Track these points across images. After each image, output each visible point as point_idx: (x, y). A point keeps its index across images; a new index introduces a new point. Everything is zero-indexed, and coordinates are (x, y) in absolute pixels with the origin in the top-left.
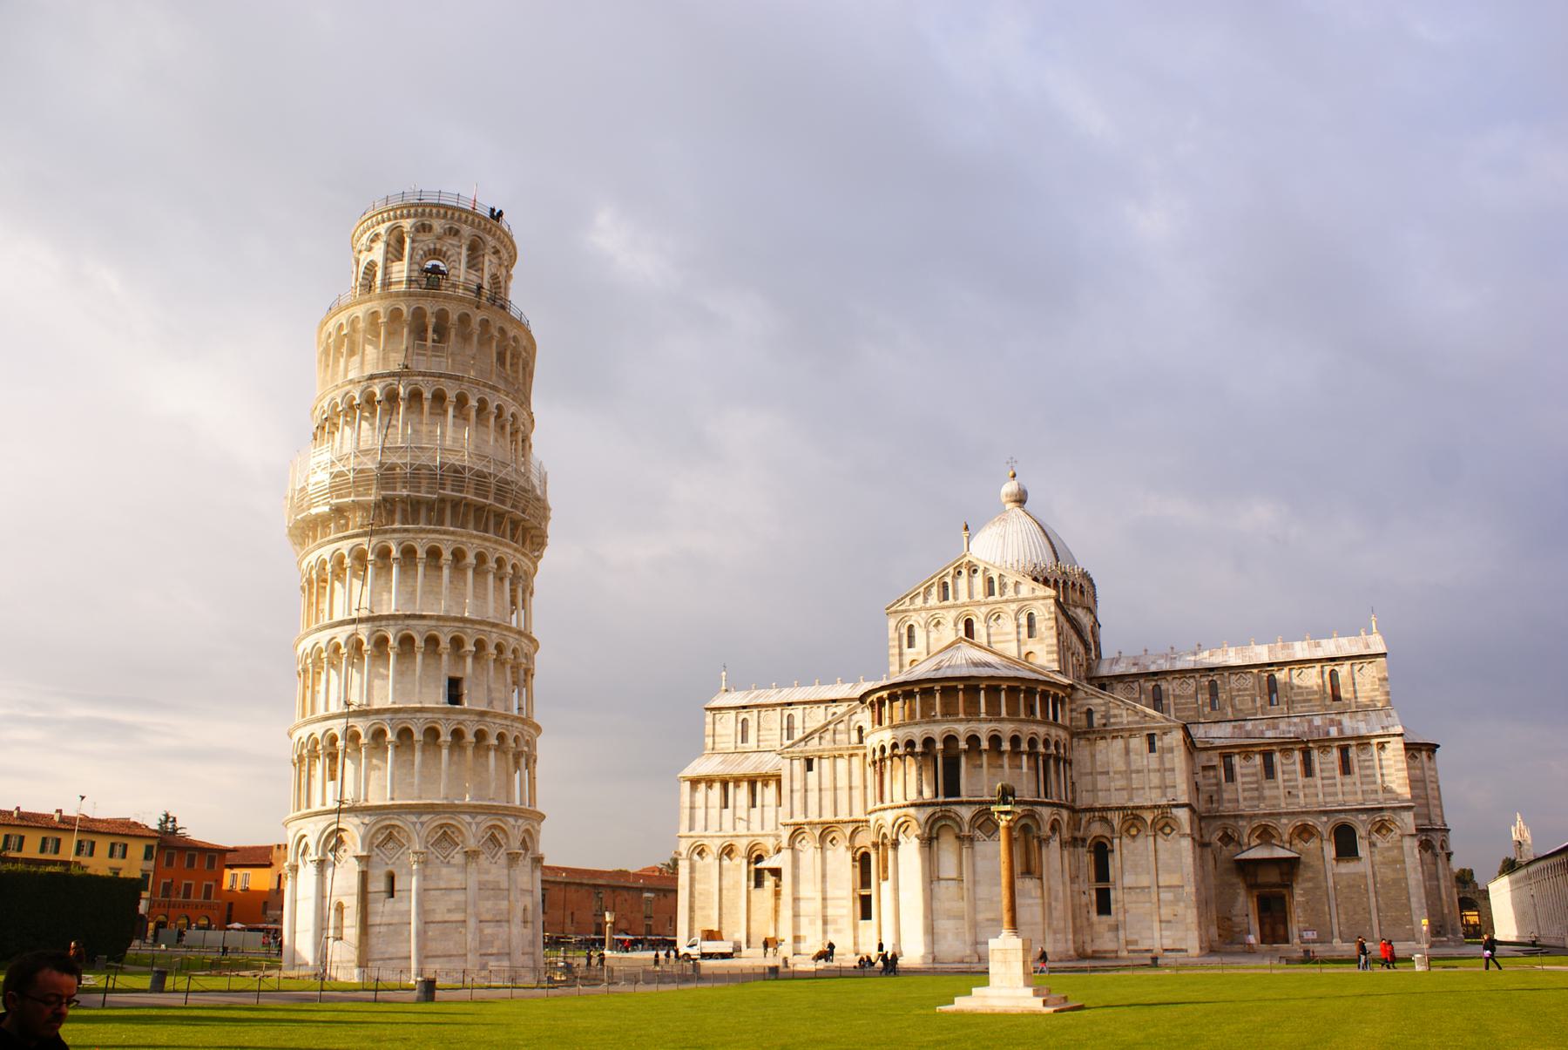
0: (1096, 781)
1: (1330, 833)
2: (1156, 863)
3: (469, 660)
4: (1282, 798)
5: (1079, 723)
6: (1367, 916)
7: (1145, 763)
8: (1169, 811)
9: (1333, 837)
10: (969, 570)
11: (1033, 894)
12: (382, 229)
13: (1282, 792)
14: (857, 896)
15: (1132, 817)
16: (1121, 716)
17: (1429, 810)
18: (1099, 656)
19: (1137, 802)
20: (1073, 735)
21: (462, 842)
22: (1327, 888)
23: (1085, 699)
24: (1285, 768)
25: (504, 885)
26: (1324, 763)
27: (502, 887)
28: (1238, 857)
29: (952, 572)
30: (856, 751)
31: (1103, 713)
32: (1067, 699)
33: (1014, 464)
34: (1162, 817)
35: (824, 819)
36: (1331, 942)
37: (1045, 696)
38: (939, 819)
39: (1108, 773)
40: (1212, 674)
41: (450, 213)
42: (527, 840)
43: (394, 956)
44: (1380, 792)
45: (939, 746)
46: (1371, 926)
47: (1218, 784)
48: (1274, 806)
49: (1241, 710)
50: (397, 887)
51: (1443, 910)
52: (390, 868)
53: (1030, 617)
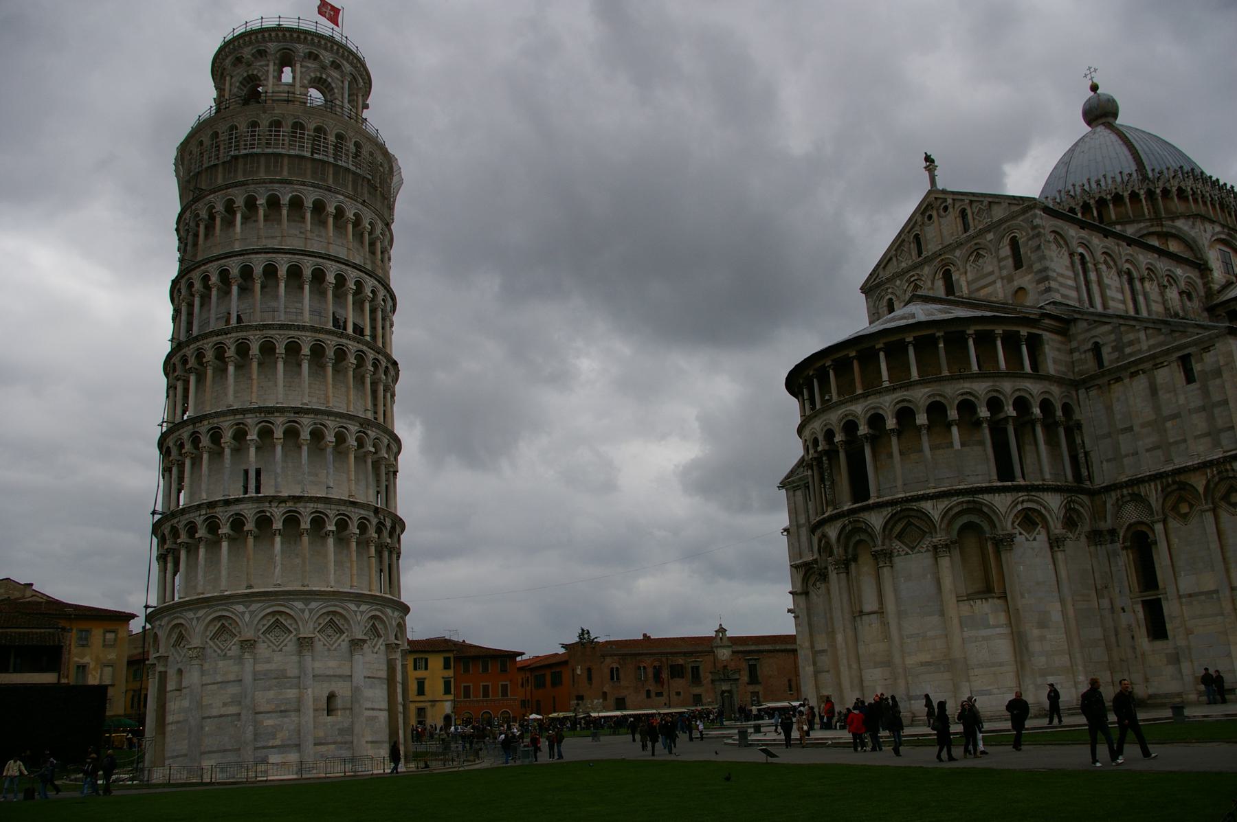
7: (1182, 400)
8: (1228, 467)
10: (938, 210)
15: (1175, 487)
16: (1138, 341)
19: (1180, 462)
20: (1076, 384)
25: (293, 671)
27: (289, 675)
31: (1114, 344)
32: (1047, 336)
34: (1221, 480)
39: (1131, 429)
52: (179, 666)
53: (1014, 244)
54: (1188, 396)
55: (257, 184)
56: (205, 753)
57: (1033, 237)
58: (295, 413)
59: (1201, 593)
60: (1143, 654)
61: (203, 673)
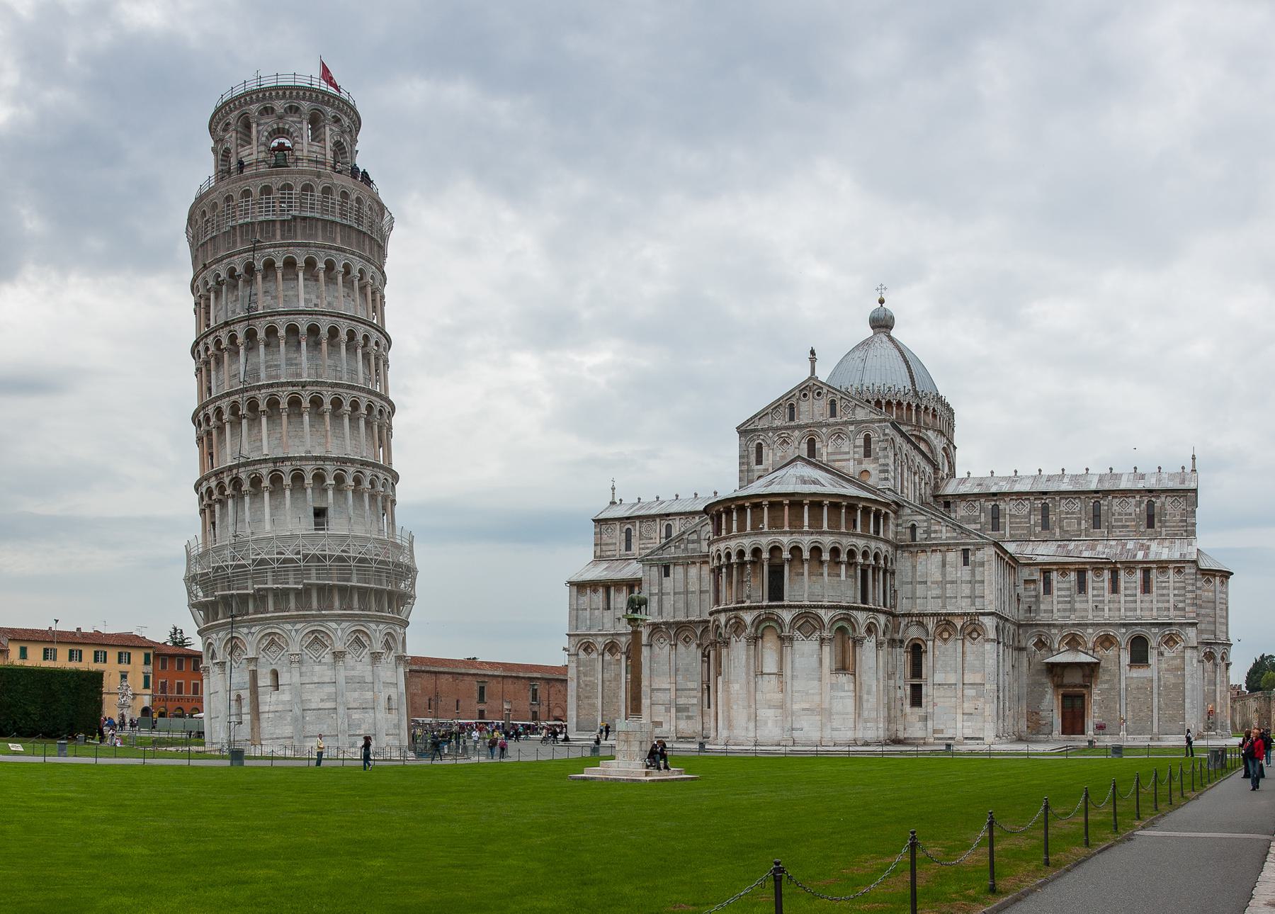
5: (904, 537)
7: (959, 575)
10: (813, 392)
16: (941, 532)
19: (950, 609)
20: (897, 547)
21: (331, 644)
23: (910, 515)
25: (369, 679)
29: (797, 394)
32: (892, 515)
35: (677, 619)
39: (925, 583)
42: (391, 641)
43: (280, 736)
52: (274, 667)
53: (867, 440)
54: (965, 573)
56: (307, 737)
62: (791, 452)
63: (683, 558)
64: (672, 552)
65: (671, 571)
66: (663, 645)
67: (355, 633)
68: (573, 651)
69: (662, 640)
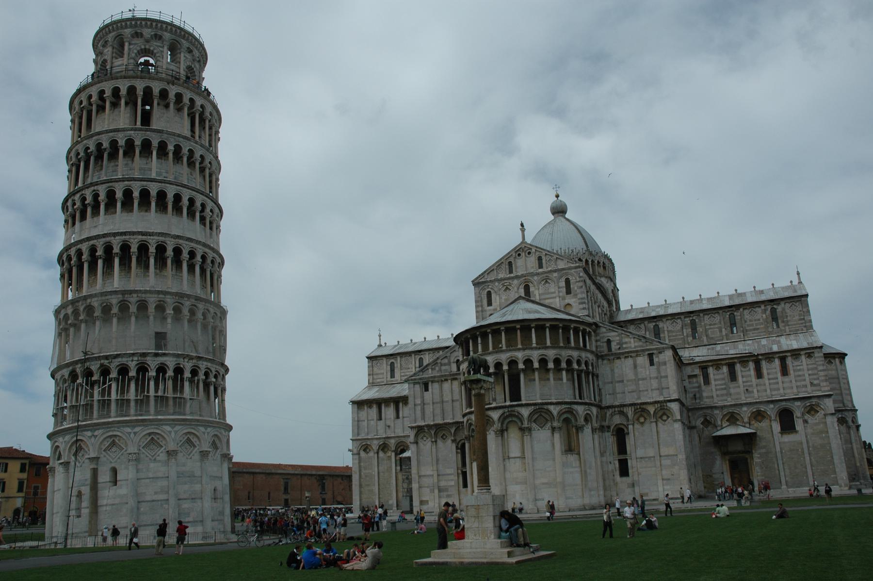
0: (615, 387)
1: (776, 415)
2: (658, 440)
3: (169, 320)
4: (743, 394)
5: (602, 349)
6: (804, 469)
7: (648, 373)
8: (665, 404)
9: (778, 418)
11: (574, 465)
12: (110, 37)
13: (742, 389)
14: (460, 472)
15: (640, 410)
16: (630, 342)
17: (843, 398)
18: (618, 308)
21: (165, 445)
22: (776, 452)
23: (605, 333)
24: (744, 374)
25: (198, 473)
26: (769, 369)
27: (196, 475)
28: (715, 434)
29: (514, 254)
30: (456, 377)
31: (618, 342)
32: (593, 333)
33: (555, 189)
34: (661, 409)
35: (437, 422)
36: (781, 489)
37: (576, 331)
38: (507, 417)
39: (622, 381)
40: (692, 315)
41: (154, 24)
42: (217, 442)
44: (809, 386)
45: (505, 367)
46: (807, 477)
47: (699, 387)
48: (737, 399)
49: (712, 338)
50: (118, 478)
51: (856, 464)
52: (113, 465)
53: (568, 282)
55: (169, 134)
57: (579, 281)
58: (196, 300)
59: (646, 458)
60: (617, 483)
61: (138, 471)
62: (513, 295)
63: (439, 377)
64: (430, 373)
65: (430, 387)
66: (427, 441)
67: (186, 435)
68: (355, 451)
69: (425, 438)
